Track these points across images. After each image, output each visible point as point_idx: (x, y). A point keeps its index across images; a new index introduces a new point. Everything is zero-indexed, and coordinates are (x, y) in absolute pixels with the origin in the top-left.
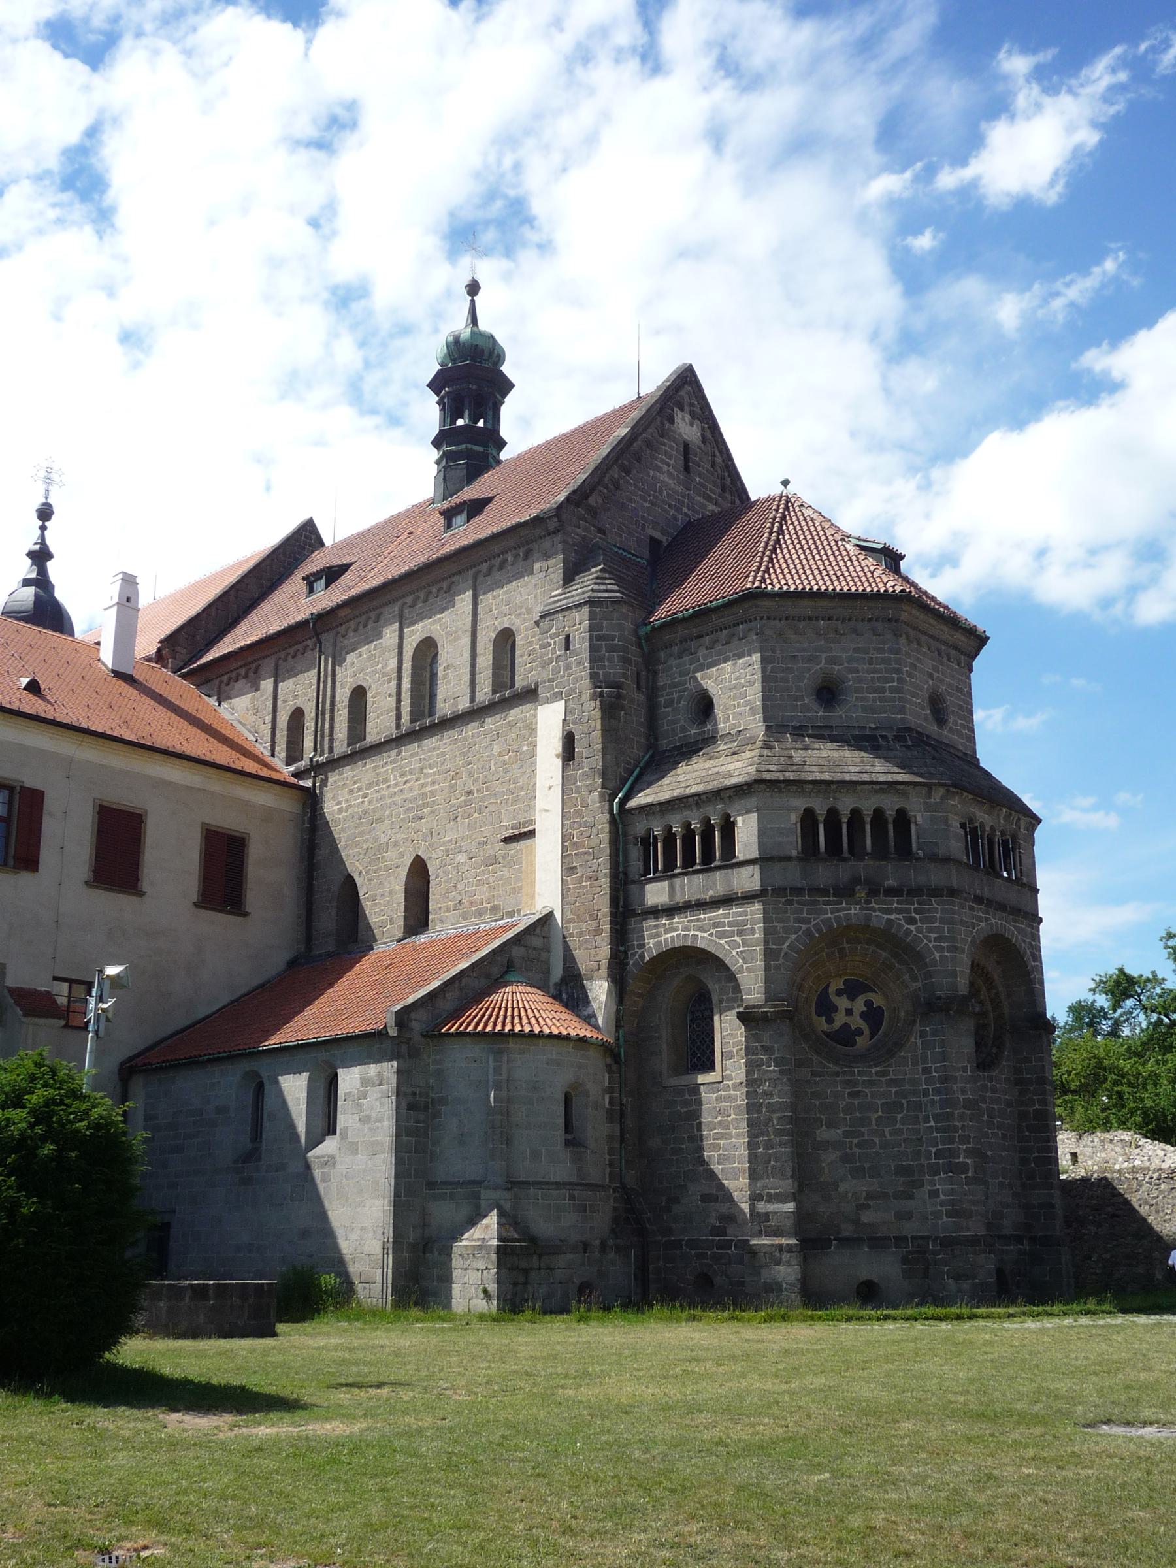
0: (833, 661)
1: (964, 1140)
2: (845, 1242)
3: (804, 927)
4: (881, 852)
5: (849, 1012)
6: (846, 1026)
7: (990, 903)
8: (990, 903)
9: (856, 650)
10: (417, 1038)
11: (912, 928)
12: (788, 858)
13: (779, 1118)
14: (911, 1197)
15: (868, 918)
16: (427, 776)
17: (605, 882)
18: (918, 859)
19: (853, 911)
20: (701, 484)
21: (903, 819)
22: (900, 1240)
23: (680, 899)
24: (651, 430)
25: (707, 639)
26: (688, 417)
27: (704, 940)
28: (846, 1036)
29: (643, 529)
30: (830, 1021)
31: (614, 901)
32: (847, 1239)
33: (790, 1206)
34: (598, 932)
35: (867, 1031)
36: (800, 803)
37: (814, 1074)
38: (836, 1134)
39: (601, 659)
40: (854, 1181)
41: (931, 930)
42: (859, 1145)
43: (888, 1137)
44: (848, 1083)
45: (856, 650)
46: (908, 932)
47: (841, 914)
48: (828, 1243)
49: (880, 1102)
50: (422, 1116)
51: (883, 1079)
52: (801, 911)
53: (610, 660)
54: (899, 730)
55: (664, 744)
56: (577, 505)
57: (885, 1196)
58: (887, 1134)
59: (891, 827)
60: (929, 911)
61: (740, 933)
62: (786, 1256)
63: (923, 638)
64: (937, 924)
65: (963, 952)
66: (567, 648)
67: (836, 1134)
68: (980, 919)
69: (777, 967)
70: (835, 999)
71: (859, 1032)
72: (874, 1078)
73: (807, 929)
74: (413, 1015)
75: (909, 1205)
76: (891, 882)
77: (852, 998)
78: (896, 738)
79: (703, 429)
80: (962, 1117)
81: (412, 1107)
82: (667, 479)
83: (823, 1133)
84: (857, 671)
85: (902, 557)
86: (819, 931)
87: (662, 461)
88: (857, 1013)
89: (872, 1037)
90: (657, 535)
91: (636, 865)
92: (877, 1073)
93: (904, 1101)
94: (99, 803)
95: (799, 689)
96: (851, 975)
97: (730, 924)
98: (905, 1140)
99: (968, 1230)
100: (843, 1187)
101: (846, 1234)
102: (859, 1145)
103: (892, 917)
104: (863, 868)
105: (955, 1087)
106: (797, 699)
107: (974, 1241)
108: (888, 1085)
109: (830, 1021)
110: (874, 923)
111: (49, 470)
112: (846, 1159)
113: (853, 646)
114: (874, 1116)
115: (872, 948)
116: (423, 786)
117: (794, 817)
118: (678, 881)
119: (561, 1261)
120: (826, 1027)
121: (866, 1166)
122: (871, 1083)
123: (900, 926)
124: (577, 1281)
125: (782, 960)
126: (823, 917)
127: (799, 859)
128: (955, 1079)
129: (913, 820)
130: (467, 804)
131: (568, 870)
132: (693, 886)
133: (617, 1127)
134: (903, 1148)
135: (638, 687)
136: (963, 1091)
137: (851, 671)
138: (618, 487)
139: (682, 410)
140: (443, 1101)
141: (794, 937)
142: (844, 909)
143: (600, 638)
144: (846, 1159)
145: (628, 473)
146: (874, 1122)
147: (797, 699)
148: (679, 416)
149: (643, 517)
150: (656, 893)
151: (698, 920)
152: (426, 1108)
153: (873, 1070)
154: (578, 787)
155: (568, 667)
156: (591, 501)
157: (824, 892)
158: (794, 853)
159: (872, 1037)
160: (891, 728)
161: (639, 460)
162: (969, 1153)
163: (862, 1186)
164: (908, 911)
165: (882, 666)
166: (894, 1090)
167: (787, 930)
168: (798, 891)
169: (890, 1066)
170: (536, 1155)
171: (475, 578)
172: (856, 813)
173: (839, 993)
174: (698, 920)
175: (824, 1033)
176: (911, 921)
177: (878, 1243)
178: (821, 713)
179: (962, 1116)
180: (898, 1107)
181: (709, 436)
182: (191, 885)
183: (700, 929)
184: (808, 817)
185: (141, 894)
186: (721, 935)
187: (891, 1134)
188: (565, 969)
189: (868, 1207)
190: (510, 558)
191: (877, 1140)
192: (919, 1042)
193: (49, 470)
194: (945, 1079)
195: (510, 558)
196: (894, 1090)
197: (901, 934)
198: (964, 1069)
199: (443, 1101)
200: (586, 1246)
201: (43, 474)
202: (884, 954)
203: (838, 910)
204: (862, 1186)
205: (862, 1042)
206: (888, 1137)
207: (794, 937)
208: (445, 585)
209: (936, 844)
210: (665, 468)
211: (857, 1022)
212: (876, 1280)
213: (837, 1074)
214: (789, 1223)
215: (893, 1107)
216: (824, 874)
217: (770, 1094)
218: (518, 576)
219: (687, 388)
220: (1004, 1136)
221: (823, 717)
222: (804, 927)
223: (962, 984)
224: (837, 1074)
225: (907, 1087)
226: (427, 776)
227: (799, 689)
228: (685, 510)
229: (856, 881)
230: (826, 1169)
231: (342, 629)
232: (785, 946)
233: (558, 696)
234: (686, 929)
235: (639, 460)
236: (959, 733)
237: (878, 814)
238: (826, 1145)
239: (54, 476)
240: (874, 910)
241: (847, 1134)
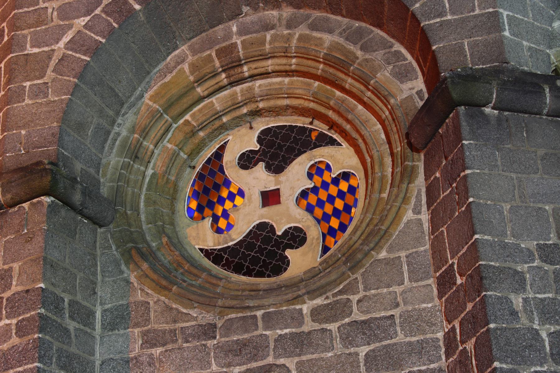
5: (270, 198)
6: (262, 226)
35: (314, 232)
37: (150, 340)
51: (333, 327)
70: (232, 171)
72: (309, 326)
77: (277, 167)
88: (289, 196)
92: (316, 313)
105: (518, 301)
108: (348, 340)
120: (211, 241)
125: (50, 74)
141: (82, 21)
153: (306, 308)
169: (351, 289)
175: (207, 253)
192: (425, 217)
196: (363, 351)
207: (82, 21)
211: (288, 215)
213: (208, 331)
224: (208, 331)
225: (401, 338)
232: (61, 44)
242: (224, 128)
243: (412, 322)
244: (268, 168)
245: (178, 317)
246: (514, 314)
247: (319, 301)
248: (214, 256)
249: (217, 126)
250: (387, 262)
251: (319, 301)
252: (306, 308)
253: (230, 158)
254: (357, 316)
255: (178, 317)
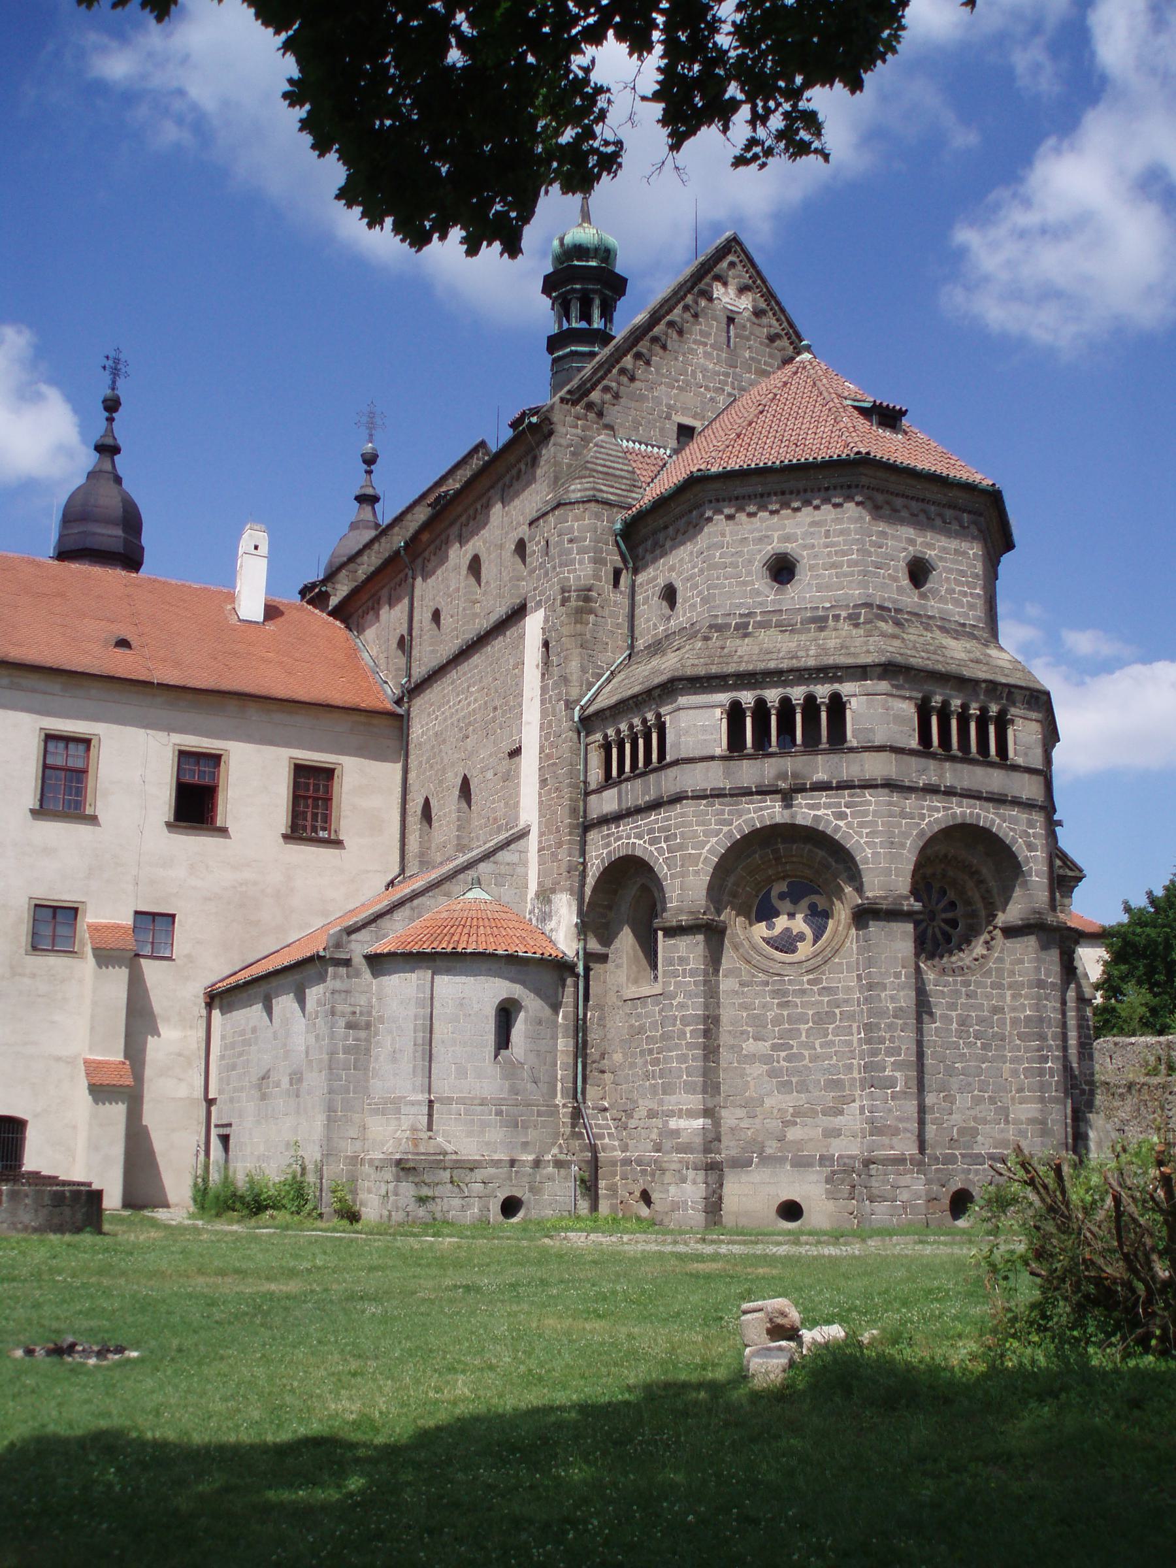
0: (787, 538)
1: (890, 1052)
2: (765, 1160)
3: (725, 829)
4: (812, 742)
6: (787, 929)
7: (950, 792)
8: (950, 792)
9: (814, 524)
10: (358, 961)
11: (841, 823)
12: (712, 758)
13: (691, 1032)
14: (841, 1113)
15: (793, 816)
16: (472, 694)
17: (566, 792)
18: (852, 750)
19: (777, 809)
20: (751, 358)
21: (837, 705)
22: (824, 1160)
23: (624, 807)
24: (678, 311)
25: (671, 530)
26: (732, 290)
27: (641, 847)
28: (786, 943)
29: (668, 417)
30: (771, 927)
31: (574, 811)
32: (769, 1157)
33: (699, 1123)
34: (559, 845)
36: (724, 698)
37: (742, 984)
38: (764, 1047)
39: (572, 562)
40: (780, 1097)
41: (862, 825)
42: (788, 1059)
43: (819, 1050)
44: (776, 993)
45: (814, 524)
46: (837, 828)
47: (765, 813)
48: (749, 1163)
49: (811, 1013)
50: (363, 1034)
51: (815, 988)
52: (722, 812)
53: (581, 562)
54: (855, 606)
55: (640, 644)
56: (575, 403)
57: (813, 1113)
58: (817, 1046)
59: (824, 715)
60: (861, 804)
61: (667, 839)
62: (691, 1174)
63: (899, 502)
64: (870, 818)
65: (903, 845)
66: (547, 554)
67: (764, 1047)
68: (937, 810)
69: (697, 873)
70: (776, 902)
71: (801, 937)
72: (806, 986)
73: (730, 831)
74: (353, 937)
75: (839, 1121)
76: (821, 776)
78: (850, 617)
79: (754, 300)
80: (890, 1027)
81: (350, 1026)
82: (702, 361)
83: (750, 1046)
84: (813, 546)
85: (903, 413)
86: (740, 830)
87: (695, 342)
89: (815, 942)
90: (688, 421)
91: (596, 774)
92: (809, 982)
93: (837, 1011)
94: (177, 748)
95: (749, 573)
96: (796, 877)
97: (661, 830)
98: (836, 1053)
99: (892, 1148)
100: (768, 1102)
101: (769, 1151)
102: (788, 1059)
103: (819, 813)
104: (789, 764)
105: (883, 995)
106: (745, 583)
107: (900, 1161)
109: (771, 927)
110: (799, 821)
111: (372, 415)
112: (772, 1074)
113: (809, 520)
114: (804, 1027)
115: (809, 847)
116: (469, 704)
117: (718, 711)
118: (624, 785)
119: (479, 1174)
120: (766, 933)
121: (794, 1080)
122: (803, 992)
123: (828, 822)
124: (502, 1196)
125: (701, 865)
126: (744, 818)
127: (723, 758)
128: (884, 987)
129: (848, 706)
130: (494, 720)
131: (543, 782)
132: (636, 792)
133: (571, 1042)
134: (834, 1061)
135: (616, 584)
136: (893, 999)
137: (805, 547)
138: (632, 379)
139: (725, 284)
140: (381, 1019)
142: (768, 808)
143: (571, 541)
144: (772, 1074)
145: (648, 363)
146: (804, 1035)
147: (745, 583)
148: (718, 290)
149: (669, 407)
150: (608, 802)
151: (637, 827)
152: (368, 1026)
153: (805, 979)
154: (551, 697)
155: (546, 574)
156: (595, 396)
157: (747, 793)
158: (718, 752)
159: (815, 942)
160: (847, 606)
161: (664, 347)
162: (897, 1066)
163: (789, 1101)
164: (839, 805)
165: (841, 539)
166: (826, 999)
167: (707, 834)
168: (717, 794)
169: (823, 973)
170: (462, 1073)
171: (503, 490)
172: (786, 702)
173: (782, 896)
174: (637, 827)
175: (764, 939)
176: (841, 816)
177: (802, 1163)
178: (772, 597)
179: (890, 1027)
180: (830, 1016)
181: (763, 305)
182: (281, 818)
183: (639, 836)
184: (735, 713)
185: (223, 831)
186: (653, 841)
187: (821, 1047)
188: (539, 884)
189: (795, 1124)
190: (523, 467)
191: (806, 1053)
192: (854, 946)
193: (372, 415)
194: (870, 987)
195: (523, 467)
196: (826, 999)
197: (829, 831)
198: (897, 975)
199: (381, 1019)
200: (512, 1163)
201: (364, 419)
202: (821, 853)
203: (761, 809)
204: (789, 1101)
205: (804, 949)
206: (819, 1050)
208: (484, 500)
209: (872, 730)
210: (701, 350)
212: (798, 1200)
214: (698, 1140)
215: (822, 1019)
216: (750, 772)
217: (682, 1006)
218: (529, 484)
219: (730, 258)
220: (985, 1047)
221: (773, 601)
222: (725, 829)
223: (902, 883)
224: (767, 984)
226: (472, 694)
227: (749, 573)
228: (728, 389)
229: (782, 776)
230: (752, 1084)
231: (426, 554)
233: (539, 605)
234: (629, 837)
235: (664, 347)
236: (958, 603)
237: (810, 699)
238: (752, 1058)
239: (378, 420)
240: (800, 806)
241: (774, 1047)
242: (774, 881)
243: (848, 990)
244: (792, 902)
245: (754, 976)
246: (880, 1001)
247: (811, 977)
248: (767, 941)
249: (770, 881)
250: (838, 963)
251: (811, 977)
252: (805, 979)
253: (774, 893)
254: (824, 984)
255: (754, 976)
